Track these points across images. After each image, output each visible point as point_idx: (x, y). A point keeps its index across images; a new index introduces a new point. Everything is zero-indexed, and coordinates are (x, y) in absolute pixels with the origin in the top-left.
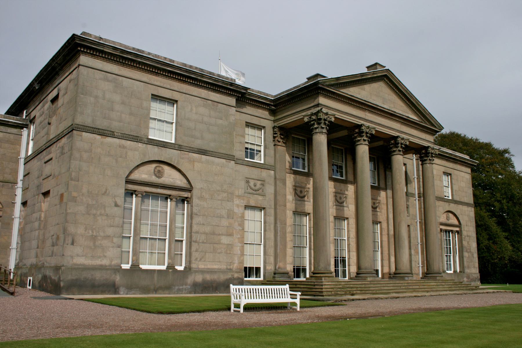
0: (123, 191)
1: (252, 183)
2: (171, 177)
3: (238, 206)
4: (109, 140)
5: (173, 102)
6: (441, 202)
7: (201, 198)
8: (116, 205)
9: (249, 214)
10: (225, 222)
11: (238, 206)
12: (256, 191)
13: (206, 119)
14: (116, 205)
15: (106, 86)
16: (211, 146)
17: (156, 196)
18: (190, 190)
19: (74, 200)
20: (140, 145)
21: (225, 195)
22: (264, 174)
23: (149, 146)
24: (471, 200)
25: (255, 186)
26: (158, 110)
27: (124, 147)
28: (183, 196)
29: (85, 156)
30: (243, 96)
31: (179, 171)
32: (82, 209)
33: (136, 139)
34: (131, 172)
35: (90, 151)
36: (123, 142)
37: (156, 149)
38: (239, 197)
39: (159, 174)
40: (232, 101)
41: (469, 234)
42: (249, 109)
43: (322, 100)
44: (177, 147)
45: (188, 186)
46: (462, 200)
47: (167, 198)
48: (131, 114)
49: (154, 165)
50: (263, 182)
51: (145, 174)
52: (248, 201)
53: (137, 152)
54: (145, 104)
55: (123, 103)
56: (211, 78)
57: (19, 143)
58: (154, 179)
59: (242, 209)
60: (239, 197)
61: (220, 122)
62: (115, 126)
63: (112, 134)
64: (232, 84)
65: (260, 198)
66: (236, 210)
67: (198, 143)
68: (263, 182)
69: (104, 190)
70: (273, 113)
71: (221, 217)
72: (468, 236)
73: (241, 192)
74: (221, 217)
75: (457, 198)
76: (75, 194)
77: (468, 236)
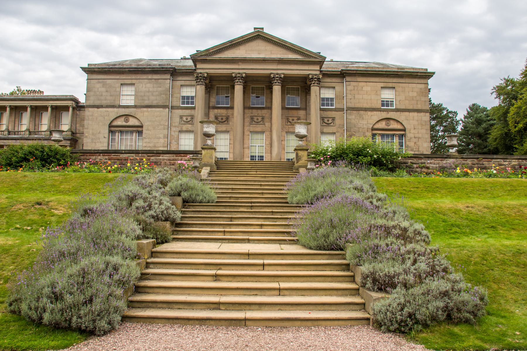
0: (107, 131)
1: (184, 119)
2: (132, 122)
3: (174, 132)
4: (101, 109)
6: (375, 112)
7: (148, 130)
8: (104, 137)
9: (183, 136)
10: (162, 141)
11: (174, 132)
12: (187, 122)
13: (151, 89)
14: (104, 137)
15: (98, 86)
16: (155, 103)
17: (127, 132)
18: (142, 127)
19: (86, 137)
20: (115, 109)
21: (163, 126)
23: (120, 109)
25: (187, 119)
27: (108, 111)
28: (139, 130)
29: (90, 117)
30: (173, 72)
31: (136, 118)
32: (90, 140)
33: (113, 107)
34: (112, 122)
35: (92, 115)
36: (107, 109)
37: (123, 109)
38: (175, 126)
39: (127, 121)
40: (168, 76)
41: (417, 135)
44: (135, 107)
45: (140, 125)
46: (411, 107)
47: (132, 132)
48: (111, 96)
49: (124, 117)
50: (192, 117)
51: (120, 122)
52: (182, 128)
53: (113, 113)
54: (118, 89)
55: (107, 91)
56: (150, 68)
58: (124, 124)
59: (177, 133)
60: (175, 126)
61: (160, 89)
62: (104, 103)
63: (101, 107)
64: (163, 68)
65: (190, 126)
66: (173, 133)
67: (147, 103)
69: (98, 131)
71: (159, 138)
72: (415, 137)
73: (177, 124)
74: (159, 138)
75: (398, 107)
76: (87, 135)
77: (415, 137)
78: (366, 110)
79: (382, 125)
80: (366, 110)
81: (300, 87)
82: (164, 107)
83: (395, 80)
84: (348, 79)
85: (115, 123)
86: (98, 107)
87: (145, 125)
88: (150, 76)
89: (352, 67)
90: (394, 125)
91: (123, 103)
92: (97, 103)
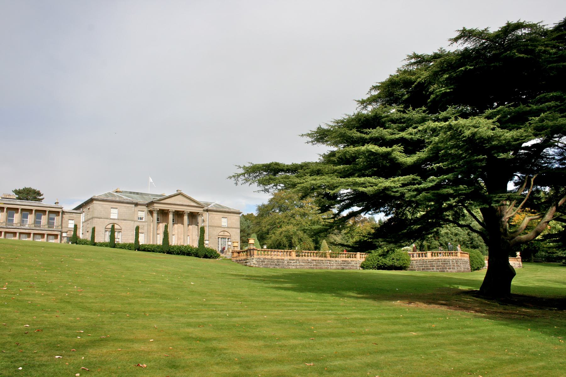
5: (116, 208)
16: (127, 218)
22: (144, 224)
24: (239, 227)
26: (113, 211)
30: (136, 204)
33: (107, 219)
40: (133, 206)
42: (139, 207)
43: (155, 205)
44: (118, 219)
50: (144, 226)
57: (80, 217)
63: (101, 218)
67: (123, 218)
68: (144, 226)
70: (147, 207)
78: (216, 227)
79: (222, 234)
80: (216, 227)
81: (193, 216)
82: (132, 220)
83: (227, 214)
84: (209, 212)
85: (107, 227)
86: (99, 218)
87: (123, 228)
88: (125, 205)
89: (210, 207)
90: (226, 234)
91: (112, 217)
92: (99, 216)
